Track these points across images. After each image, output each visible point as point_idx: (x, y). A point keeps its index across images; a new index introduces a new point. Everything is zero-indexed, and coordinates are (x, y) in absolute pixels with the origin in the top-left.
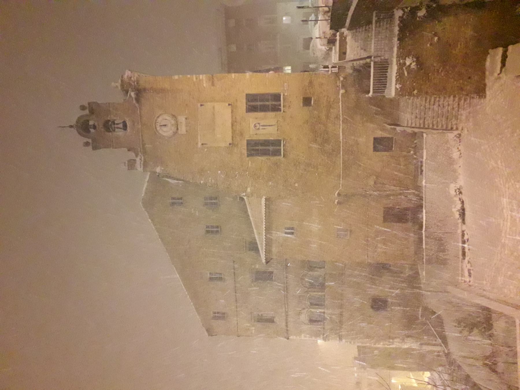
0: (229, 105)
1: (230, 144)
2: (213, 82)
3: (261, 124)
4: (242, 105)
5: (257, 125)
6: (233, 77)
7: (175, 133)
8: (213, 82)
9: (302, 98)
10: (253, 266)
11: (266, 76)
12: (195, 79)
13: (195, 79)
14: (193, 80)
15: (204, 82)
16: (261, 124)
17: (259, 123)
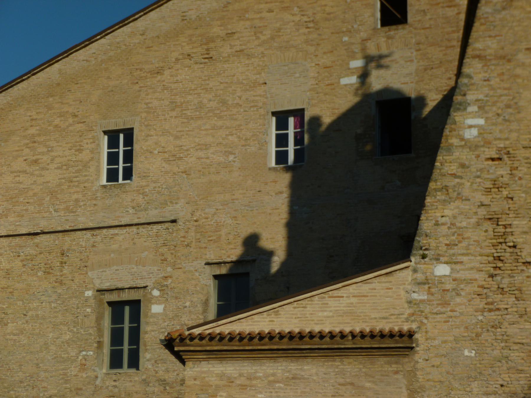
10: (156, 293)
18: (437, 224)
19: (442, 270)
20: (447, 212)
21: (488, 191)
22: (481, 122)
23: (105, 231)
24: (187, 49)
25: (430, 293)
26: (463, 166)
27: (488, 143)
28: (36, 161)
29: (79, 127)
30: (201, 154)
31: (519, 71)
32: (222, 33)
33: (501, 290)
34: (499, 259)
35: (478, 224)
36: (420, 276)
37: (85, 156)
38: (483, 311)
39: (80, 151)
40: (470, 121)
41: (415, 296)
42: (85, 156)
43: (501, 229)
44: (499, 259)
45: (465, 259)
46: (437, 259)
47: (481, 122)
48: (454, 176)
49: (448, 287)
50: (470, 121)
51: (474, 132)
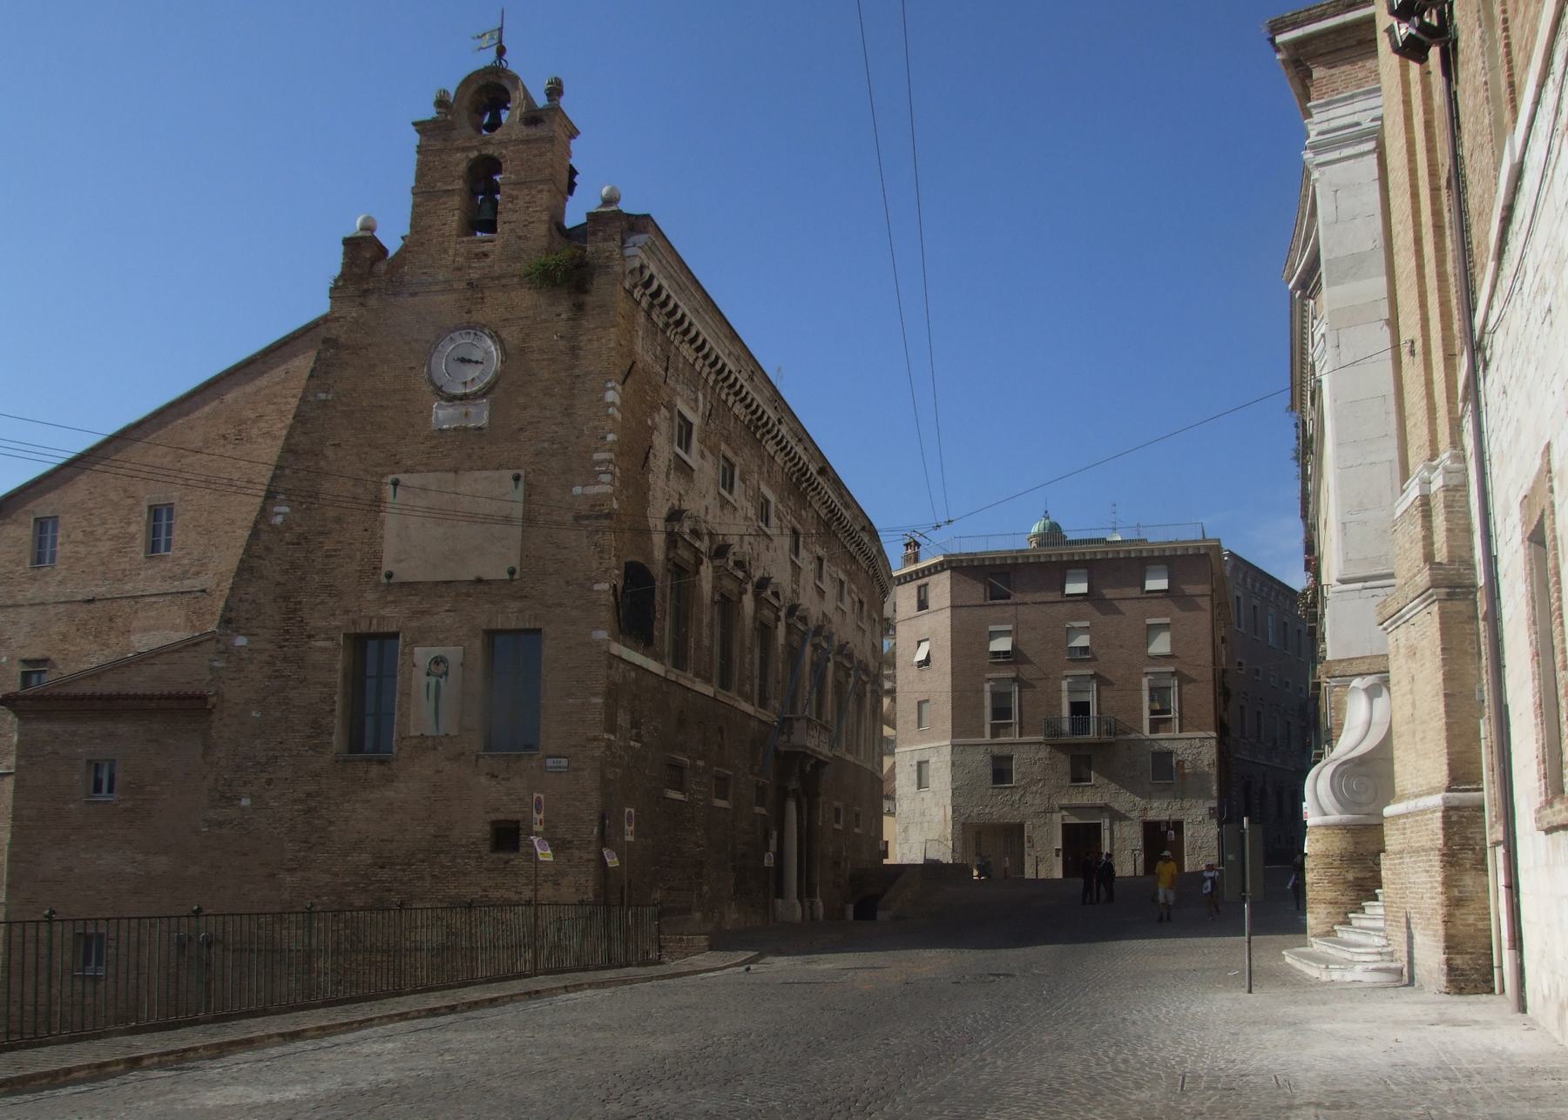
0: (512, 572)
1: (389, 575)
2: (587, 517)
3: (442, 681)
4: (510, 617)
5: (442, 667)
6: (597, 587)
7: (439, 391)
8: (587, 517)
9: (519, 816)
11: (595, 695)
12: (598, 456)
13: (598, 456)
14: (596, 450)
15: (594, 490)
16: (442, 681)
17: (446, 674)
18: (240, 600)
19: (241, 641)
20: (251, 590)
21: (286, 572)
22: (285, 509)
23: (147, 600)
24: (222, 431)
25: (228, 661)
26: (268, 549)
27: (289, 528)
28: (92, 533)
29: (130, 501)
30: (227, 528)
31: (322, 463)
32: (253, 416)
33: (285, 659)
34: (287, 632)
35: (275, 600)
36: (221, 647)
37: (133, 529)
38: (270, 677)
39: (129, 524)
40: (276, 509)
41: (216, 664)
42: (133, 529)
43: (291, 605)
44: (287, 632)
45: (260, 631)
46: (237, 631)
47: (285, 509)
48: (259, 557)
49: (244, 656)
50: (276, 509)
51: (279, 520)
